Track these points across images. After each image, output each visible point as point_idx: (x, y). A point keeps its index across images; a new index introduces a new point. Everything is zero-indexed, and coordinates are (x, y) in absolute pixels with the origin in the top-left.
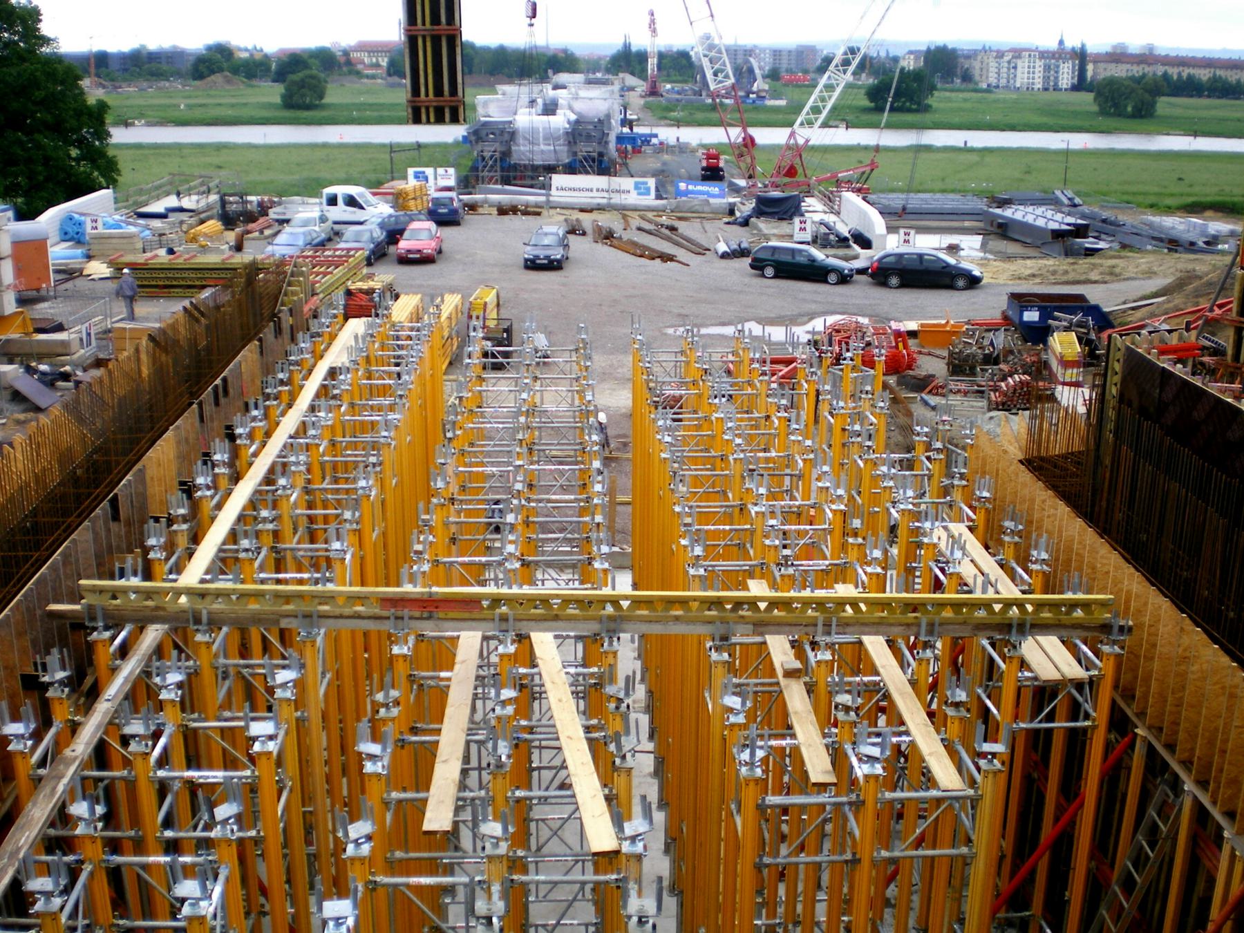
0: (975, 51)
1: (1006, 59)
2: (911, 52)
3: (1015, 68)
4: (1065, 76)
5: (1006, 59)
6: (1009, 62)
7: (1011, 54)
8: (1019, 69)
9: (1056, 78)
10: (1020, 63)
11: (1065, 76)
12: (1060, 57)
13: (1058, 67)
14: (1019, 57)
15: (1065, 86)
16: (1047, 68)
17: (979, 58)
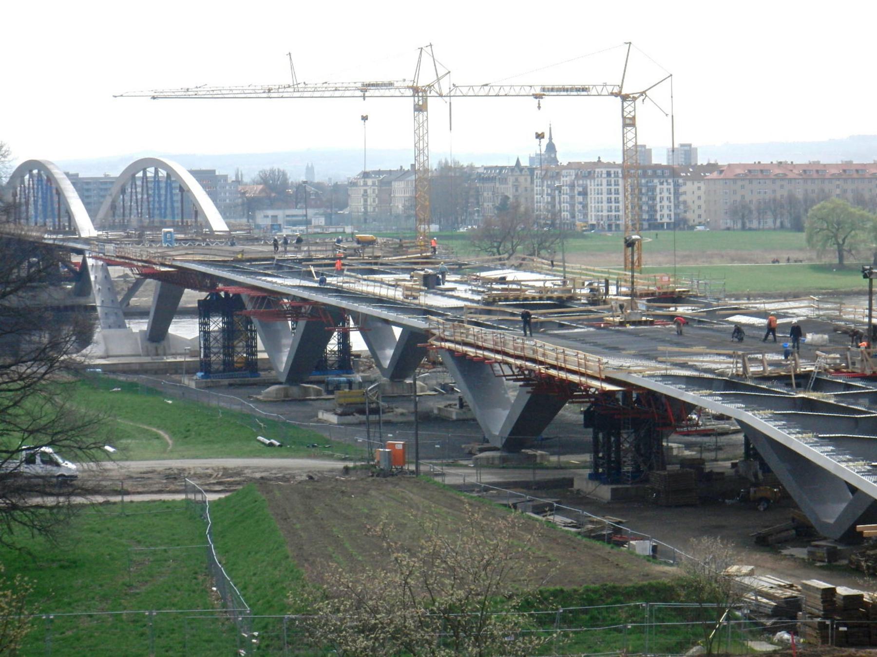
0: (502, 168)
1: (565, 180)
2: (366, 175)
3: (584, 193)
4: (665, 203)
5: (565, 180)
6: (572, 186)
7: (573, 172)
8: (592, 196)
9: (652, 209)
10: (591, 186)
11: (665, 203)
12: (655, 175)
13: (653, 189)
14: (590, 175)
15: (666, 220)
16: (637, 192)
17: (511, 180)
